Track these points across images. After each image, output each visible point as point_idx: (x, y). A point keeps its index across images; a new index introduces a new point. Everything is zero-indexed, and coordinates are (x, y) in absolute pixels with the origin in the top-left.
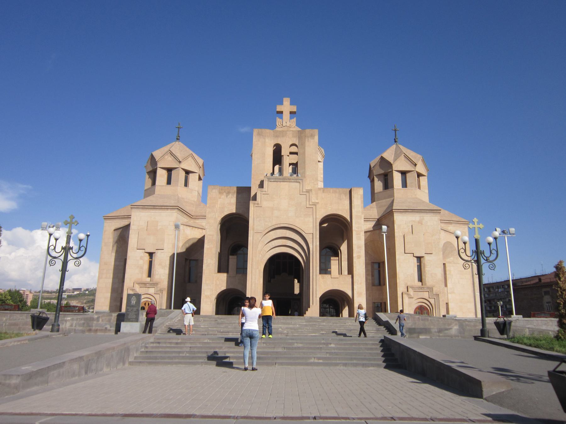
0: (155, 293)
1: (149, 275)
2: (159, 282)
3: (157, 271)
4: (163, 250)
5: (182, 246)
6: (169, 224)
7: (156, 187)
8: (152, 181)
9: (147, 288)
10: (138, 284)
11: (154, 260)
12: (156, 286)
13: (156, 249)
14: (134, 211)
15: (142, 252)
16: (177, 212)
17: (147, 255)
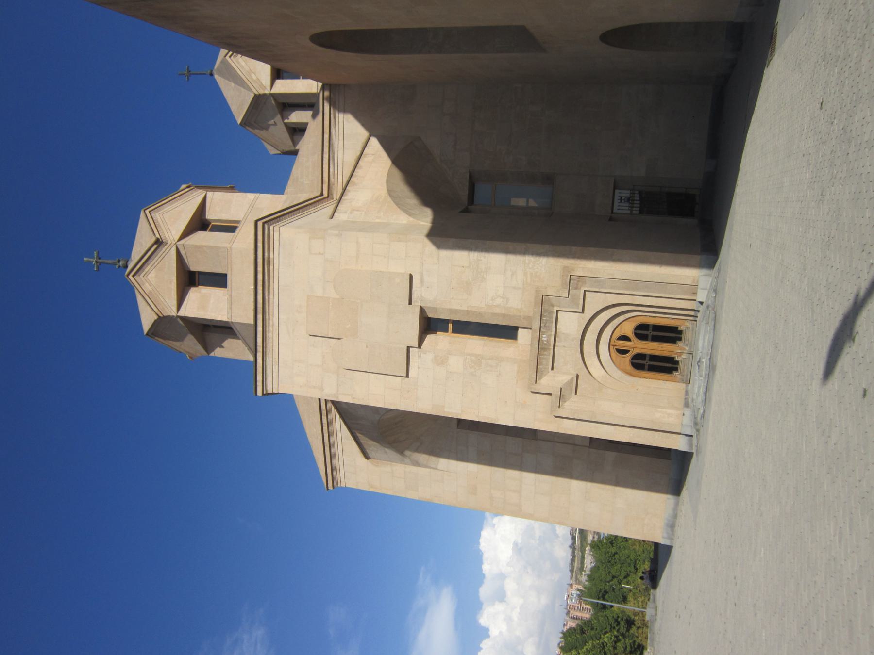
0: (581, 311)
1: (508, 332)
2: (537, 291)
3: (493, 300)
4: (411, 277)
5: (410, 215)
6: (320, 254)
7: (235, 319)
8: (231, 338)
9: (557, 344)
10: (538, 375)
11: (451, 311)
12: (553, 306)
13: (410, 303)
14: (275, 386)
15: (420, 356)
16: (276, 229)
17: (430, 338)
